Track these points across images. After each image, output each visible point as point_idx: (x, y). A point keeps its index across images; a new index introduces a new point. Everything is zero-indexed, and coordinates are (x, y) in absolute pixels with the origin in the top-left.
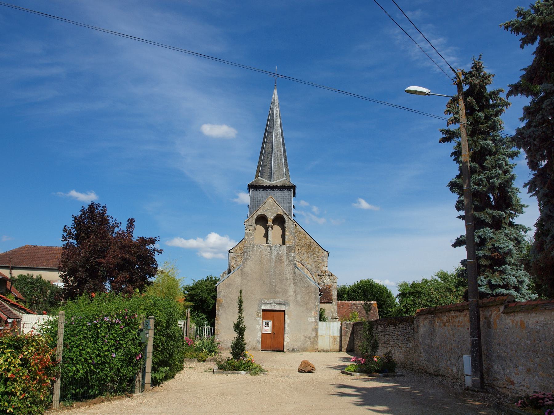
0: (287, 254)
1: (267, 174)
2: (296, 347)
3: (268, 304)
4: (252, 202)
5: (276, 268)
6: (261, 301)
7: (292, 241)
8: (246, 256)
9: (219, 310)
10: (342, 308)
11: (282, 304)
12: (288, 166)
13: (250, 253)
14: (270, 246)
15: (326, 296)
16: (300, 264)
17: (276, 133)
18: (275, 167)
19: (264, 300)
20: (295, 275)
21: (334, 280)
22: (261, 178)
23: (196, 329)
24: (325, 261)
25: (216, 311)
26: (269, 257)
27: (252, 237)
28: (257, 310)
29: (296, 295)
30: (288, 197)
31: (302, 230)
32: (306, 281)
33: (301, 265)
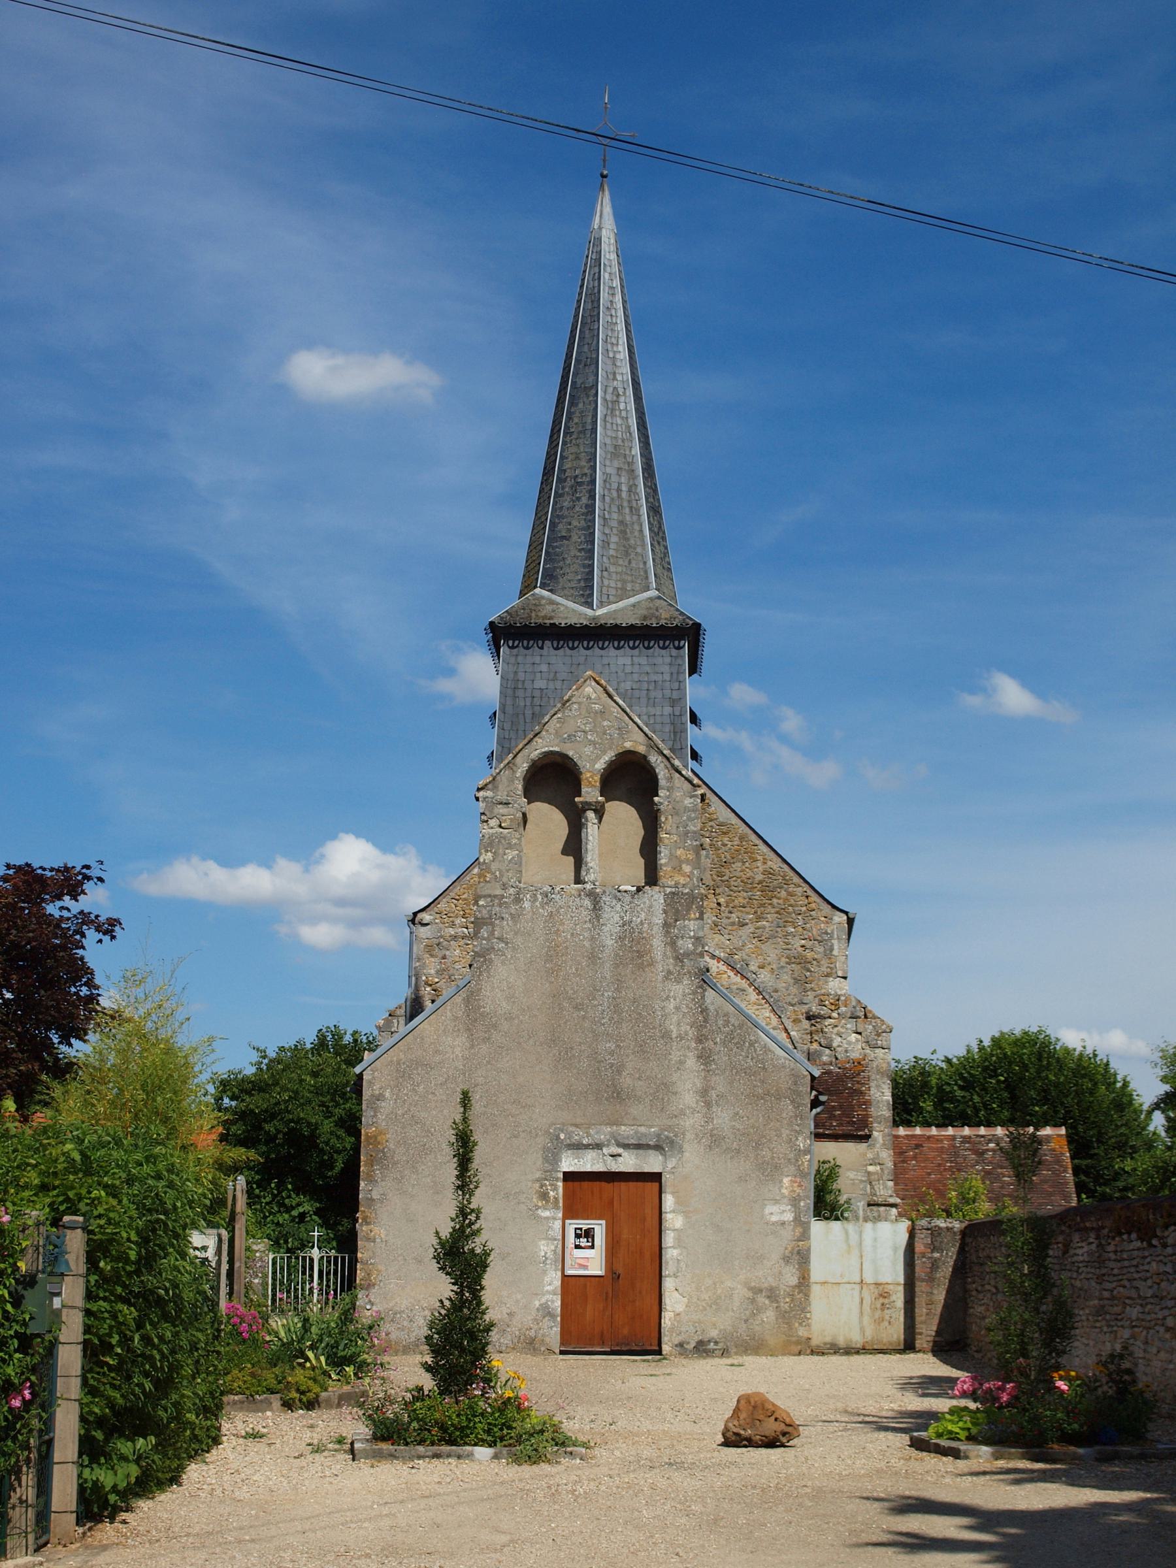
0: (666, 925)
1: (572, 573)
2: (714, 1333)
4: (509, 701)
5: (618, 990)
6: (558, 1137)
7: (687, 869)
8: (488, 939)
9: (371, 1180)
10: (915, 1157)
11: (647, 1147)
12: (664, 538)
13: (505, 927)
14: (592, 894)
15: (841, 1107)
16: (724, 968)
17: (610, 390)
18: (606, 544)
19: (571, 1129)
20: (706, 1021)
21: (878, 1035)
22: (545, 593)
23: (274, 1263)
24: (835, 952)
25: (362, 1184)
26: (587, 944)
27: (511, 854)
28: (538, 1175)
29: (708, 1105)
30: (667, 677)
31: (735, 820)
32: (751, 1044)
33: (731, 974)
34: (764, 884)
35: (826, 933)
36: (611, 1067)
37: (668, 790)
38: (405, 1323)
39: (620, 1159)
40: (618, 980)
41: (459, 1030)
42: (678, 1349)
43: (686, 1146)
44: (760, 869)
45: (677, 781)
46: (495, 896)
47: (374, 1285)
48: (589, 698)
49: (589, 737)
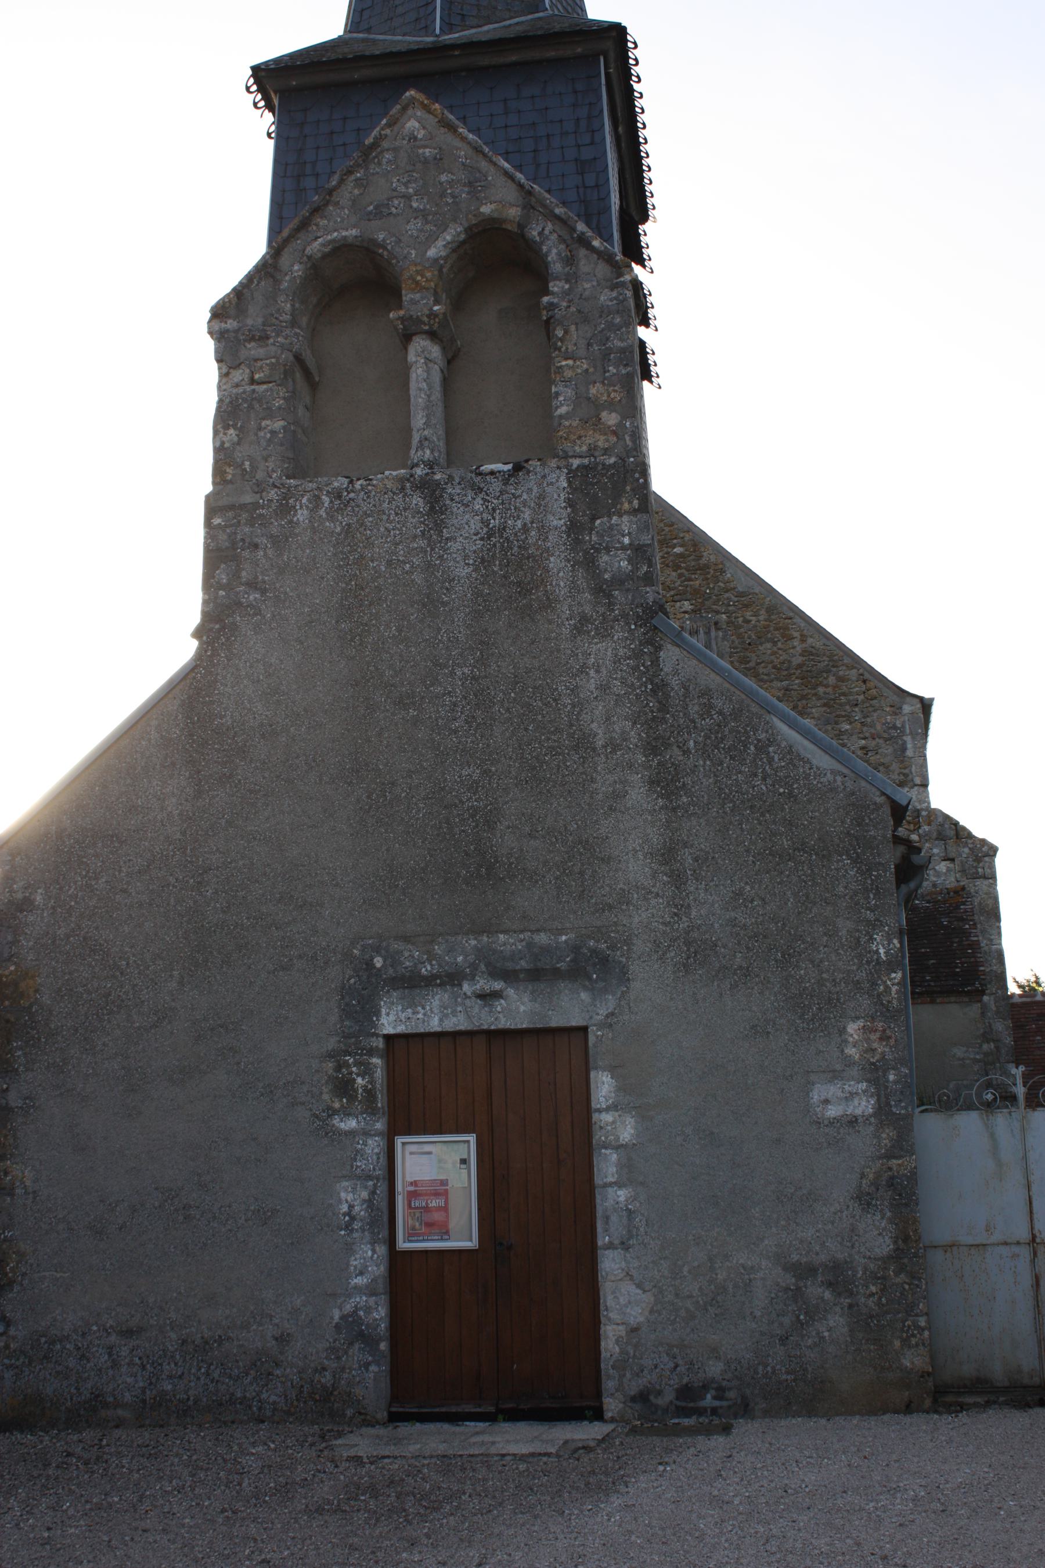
0: (574, 528)
2: (715, 1369)
3: (430, 982)
6: (370, 964)
11: (556, 974)
19: (396, 946)
20: (663, 708)
26: (418, 578)
28: (332, 1043)
29: (678, 879)
32: (762, 748)
34: (805, 668)
35: (895, 727)
36: (473, 816)
37: (567, 281)
38: (72, 1363)
39: (500, 1005)
40: (482, 642)
41: (173, 764)
42: (638, 1406)
43: (634, 968)
44: (798, 649)
45: (583, 262)
46: (243, 507)
47: (11, 1283)
48: (413, 138)
49: (415, 205)
